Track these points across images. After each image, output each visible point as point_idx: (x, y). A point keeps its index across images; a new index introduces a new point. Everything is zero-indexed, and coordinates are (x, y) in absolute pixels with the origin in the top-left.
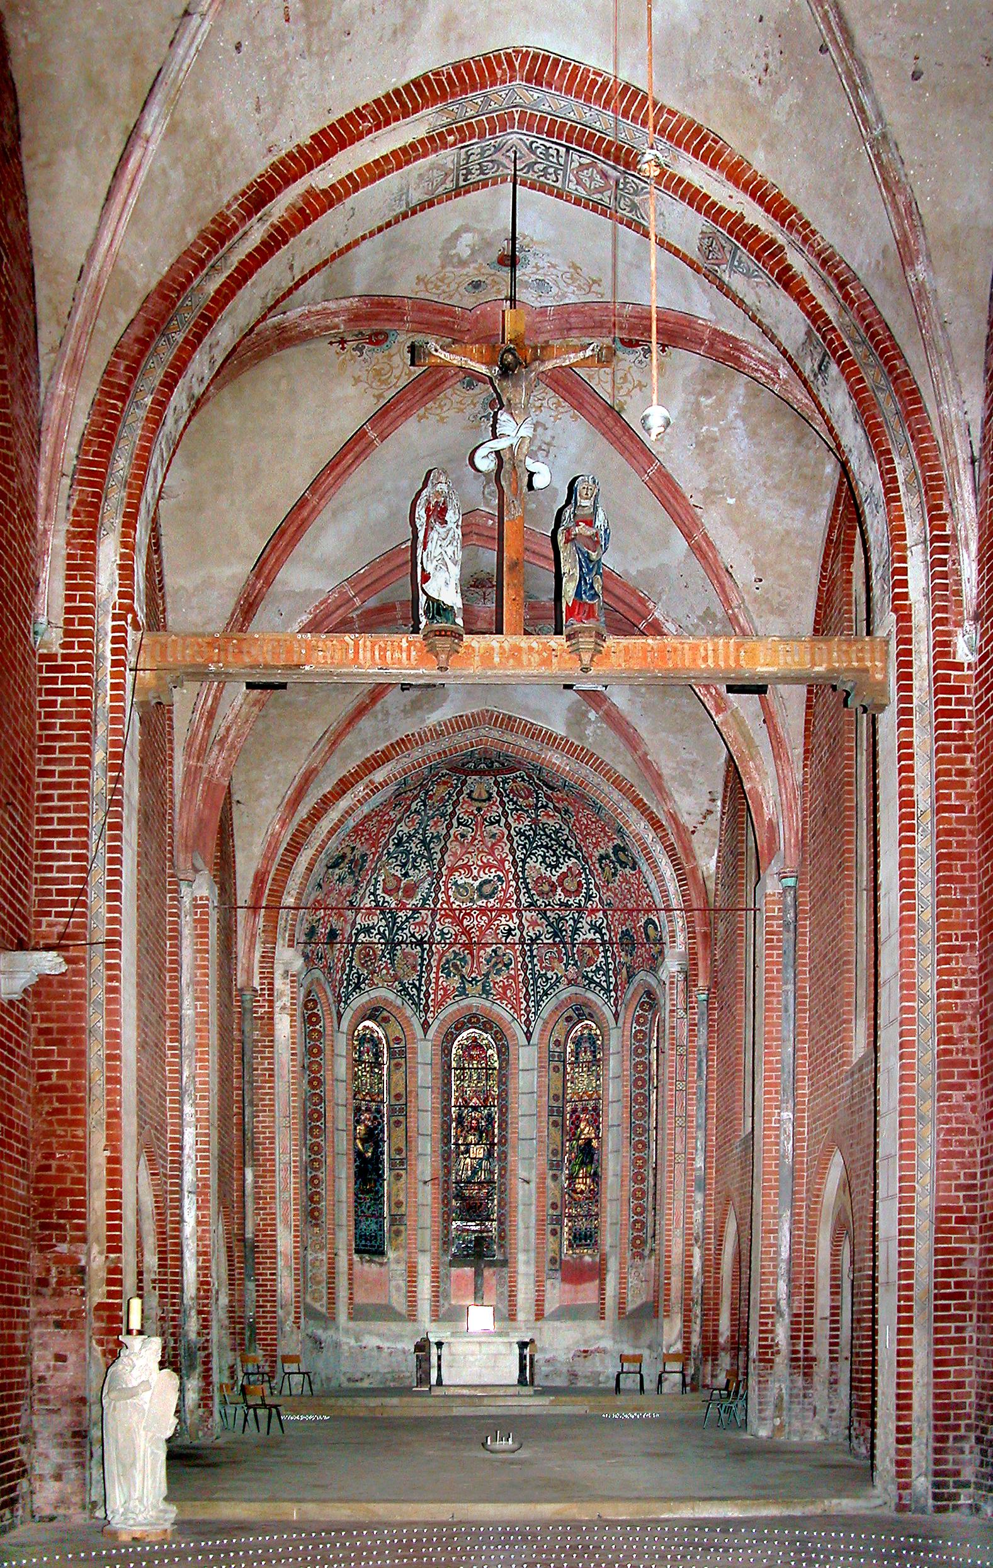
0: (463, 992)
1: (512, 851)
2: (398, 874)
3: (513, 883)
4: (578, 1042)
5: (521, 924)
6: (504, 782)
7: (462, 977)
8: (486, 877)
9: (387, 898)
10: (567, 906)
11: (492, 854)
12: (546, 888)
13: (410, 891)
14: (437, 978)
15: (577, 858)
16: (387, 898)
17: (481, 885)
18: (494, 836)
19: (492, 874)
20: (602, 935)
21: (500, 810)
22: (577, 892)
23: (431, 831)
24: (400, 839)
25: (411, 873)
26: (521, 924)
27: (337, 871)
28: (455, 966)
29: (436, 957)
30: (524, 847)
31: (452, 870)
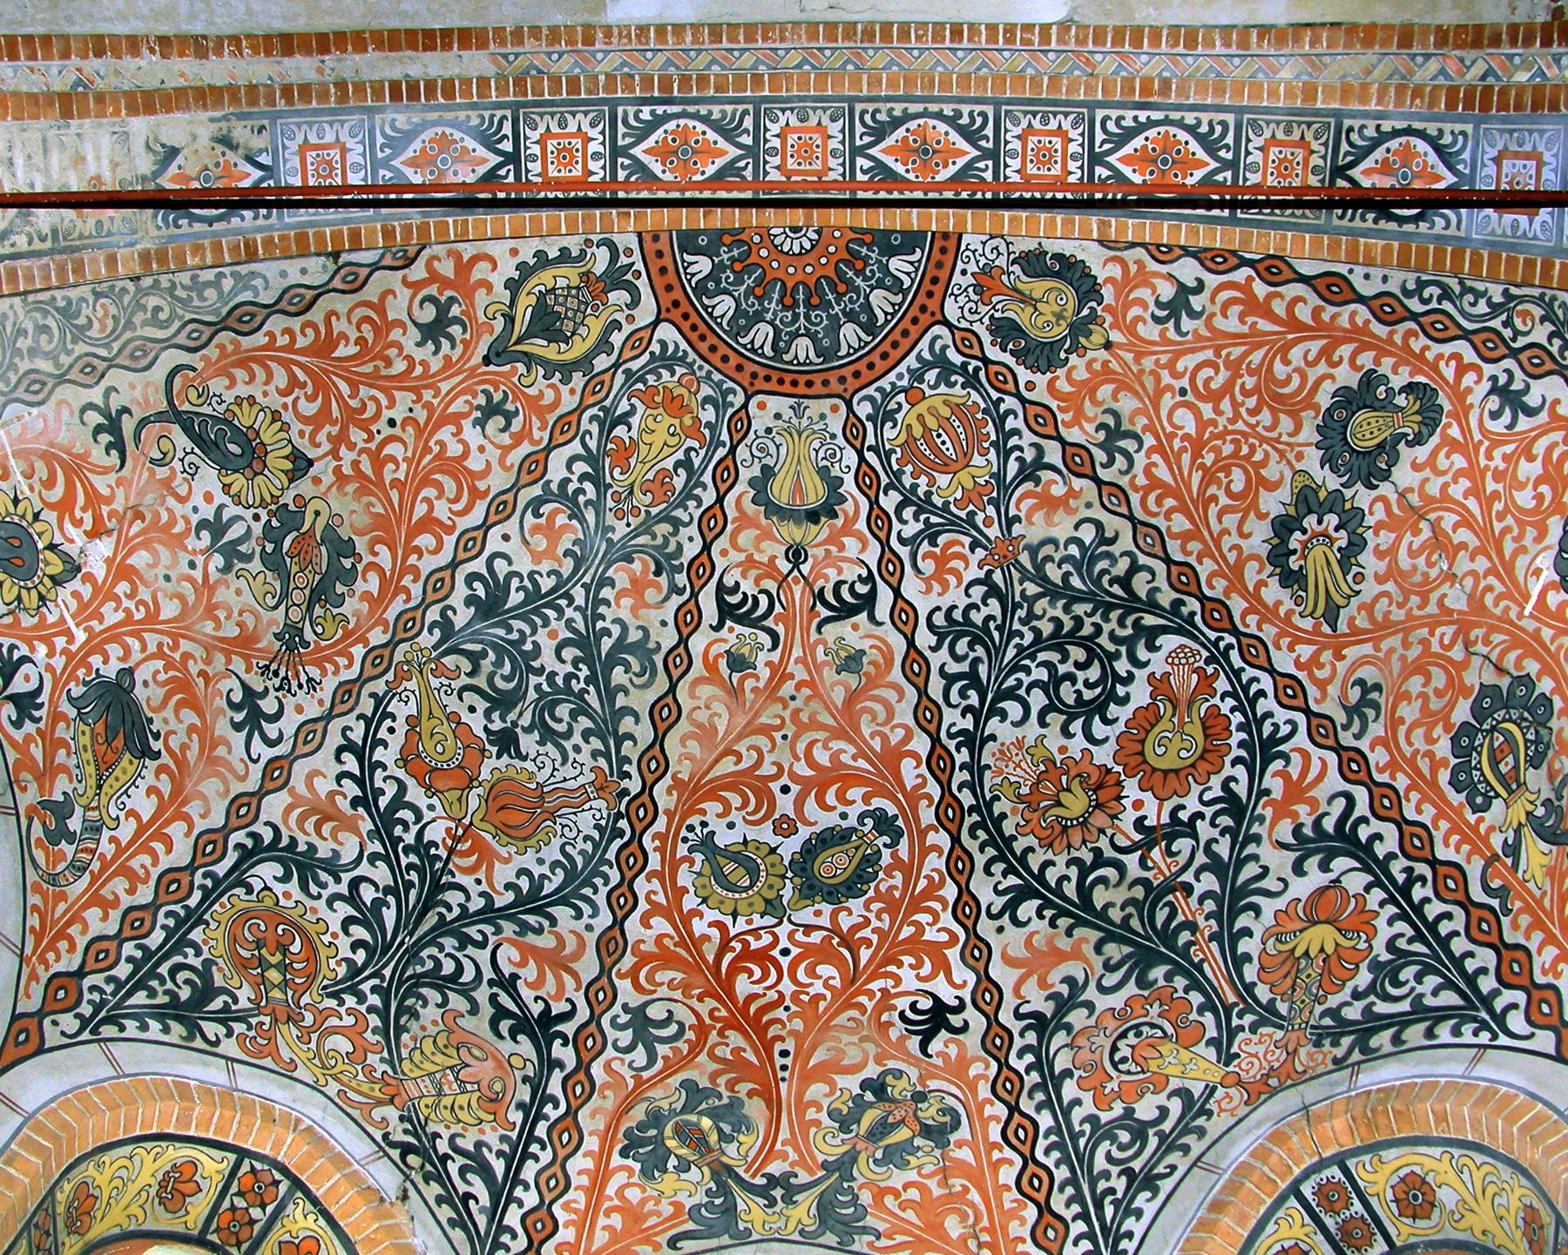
1: (927, 715)
2: (476, 723)
3: (942, 839)
5: (986, 982)
6: (883, 416)
7: (723, 1173)
9: (415, 794)
10: (1181, 827)
11: (846, 728)
12: (1076, 803)
13: (520, 811)
14: (600, 1177)
15: (1185, 627)
16: (415, 794)
17: (810, 851)
18: (852, 661)
20: (1363, 853)
21: (872, 555)
22: (1210, 756)
24: (498, 591)
25: (528, 743)
26: (984, 979)
27: (209, 477)
28: (689, 1135)
29: (604, 1102)
30: (972, 677)
31: (695, 792)
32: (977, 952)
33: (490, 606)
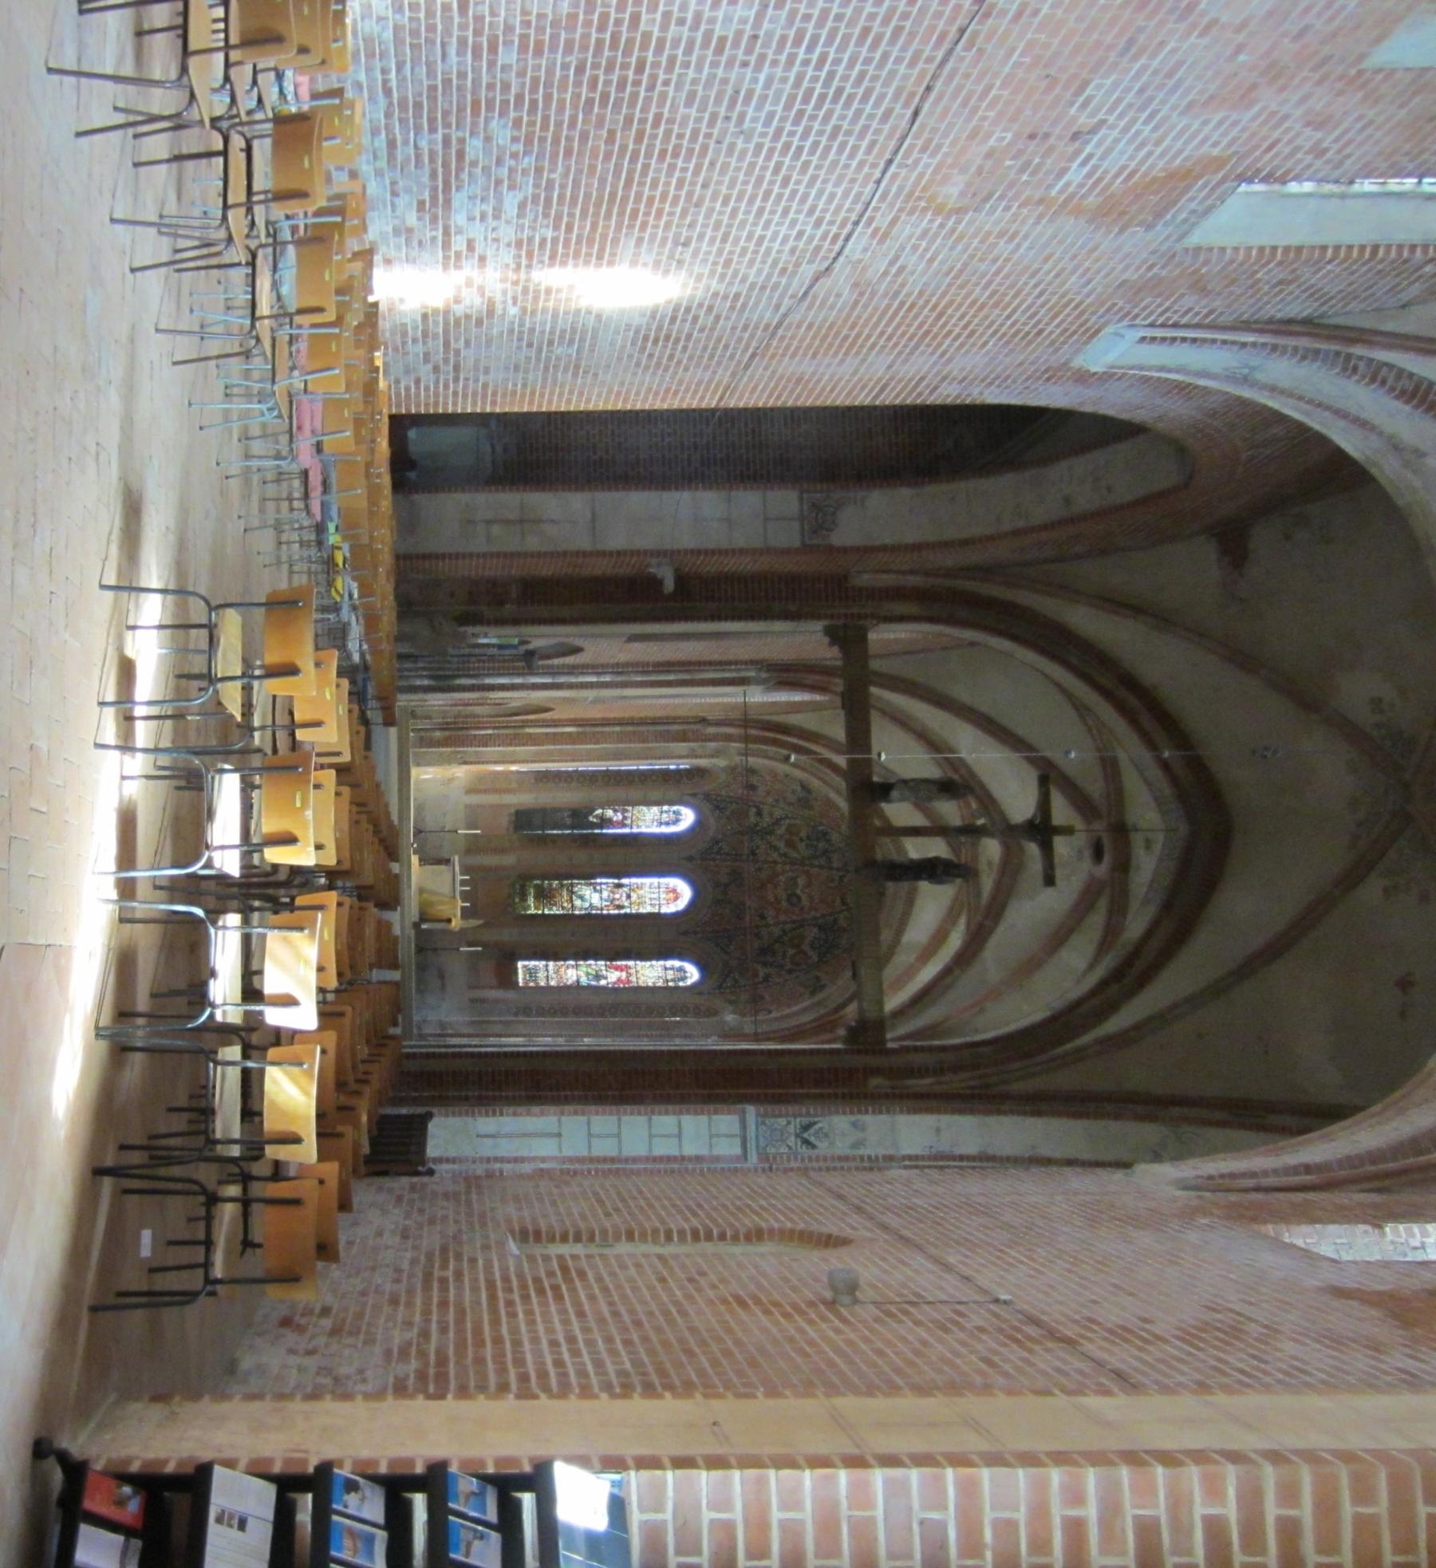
0: (717, 885)
4: (681, 969)
8: (804, 897)
13: (790, 844)
19: (805, 902)
23: (835, 857)
31: (807, 873)
32: (776, 924)
33: (825, 834)
